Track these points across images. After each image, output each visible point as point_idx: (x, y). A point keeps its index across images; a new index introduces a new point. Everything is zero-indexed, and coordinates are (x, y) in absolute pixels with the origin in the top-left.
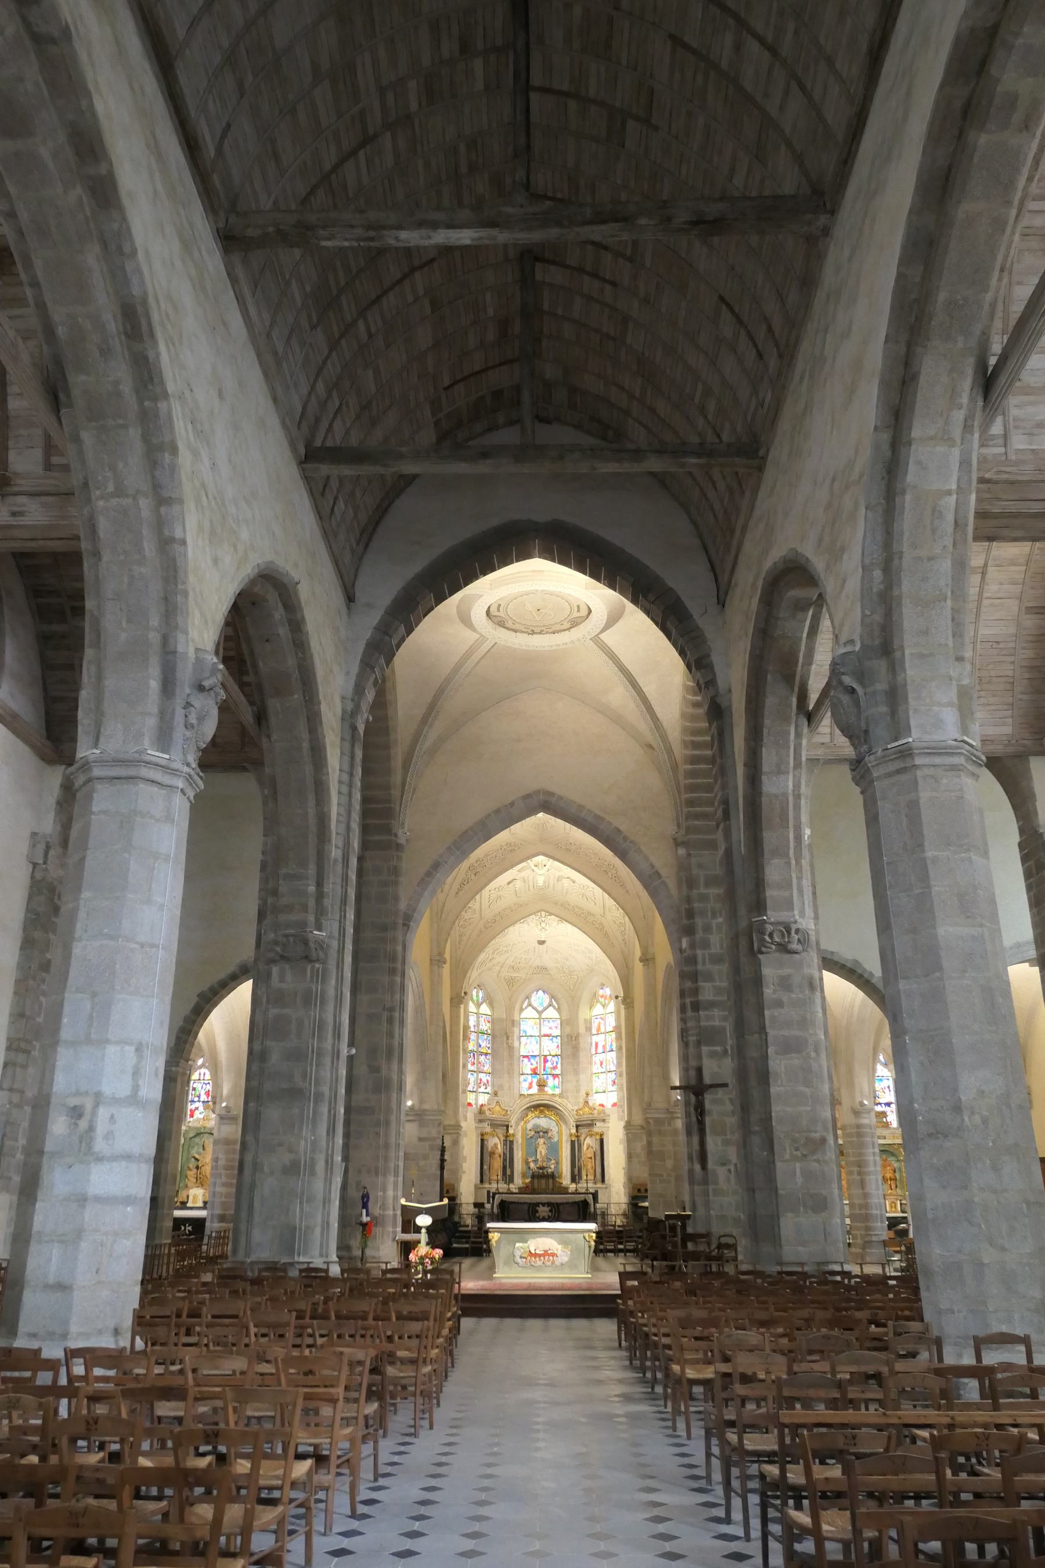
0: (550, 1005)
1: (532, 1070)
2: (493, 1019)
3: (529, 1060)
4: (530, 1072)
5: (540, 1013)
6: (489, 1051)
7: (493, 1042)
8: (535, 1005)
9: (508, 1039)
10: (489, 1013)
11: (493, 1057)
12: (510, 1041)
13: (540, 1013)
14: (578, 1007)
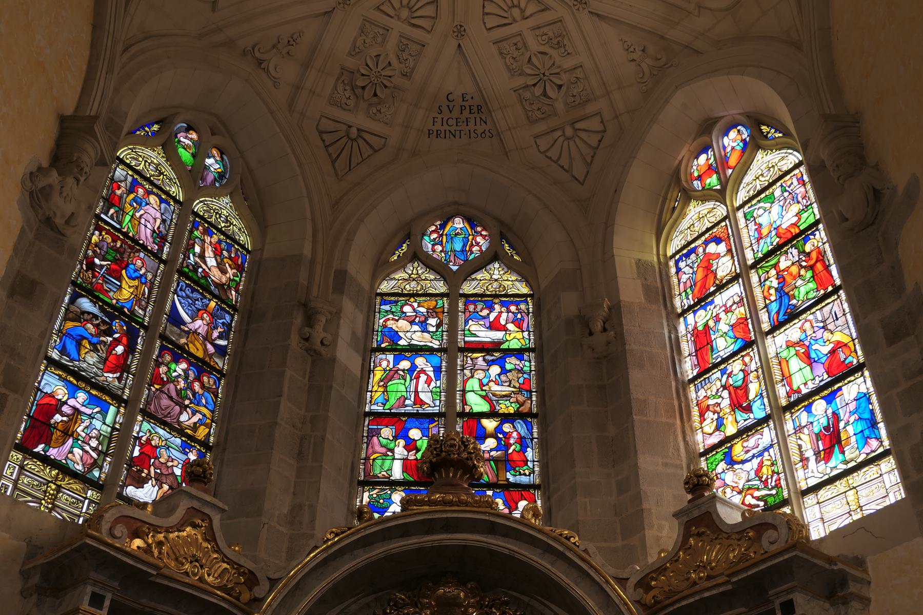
1: (407, 465)
2: (257, 265)
3: (401, 434)
4: (397, 473)
5: (453, 280)
6: (219, 363)
7: (244, 334)
9: (310, 320)
11: (233, 390)
12: (319, 333)
13: (453, 280)
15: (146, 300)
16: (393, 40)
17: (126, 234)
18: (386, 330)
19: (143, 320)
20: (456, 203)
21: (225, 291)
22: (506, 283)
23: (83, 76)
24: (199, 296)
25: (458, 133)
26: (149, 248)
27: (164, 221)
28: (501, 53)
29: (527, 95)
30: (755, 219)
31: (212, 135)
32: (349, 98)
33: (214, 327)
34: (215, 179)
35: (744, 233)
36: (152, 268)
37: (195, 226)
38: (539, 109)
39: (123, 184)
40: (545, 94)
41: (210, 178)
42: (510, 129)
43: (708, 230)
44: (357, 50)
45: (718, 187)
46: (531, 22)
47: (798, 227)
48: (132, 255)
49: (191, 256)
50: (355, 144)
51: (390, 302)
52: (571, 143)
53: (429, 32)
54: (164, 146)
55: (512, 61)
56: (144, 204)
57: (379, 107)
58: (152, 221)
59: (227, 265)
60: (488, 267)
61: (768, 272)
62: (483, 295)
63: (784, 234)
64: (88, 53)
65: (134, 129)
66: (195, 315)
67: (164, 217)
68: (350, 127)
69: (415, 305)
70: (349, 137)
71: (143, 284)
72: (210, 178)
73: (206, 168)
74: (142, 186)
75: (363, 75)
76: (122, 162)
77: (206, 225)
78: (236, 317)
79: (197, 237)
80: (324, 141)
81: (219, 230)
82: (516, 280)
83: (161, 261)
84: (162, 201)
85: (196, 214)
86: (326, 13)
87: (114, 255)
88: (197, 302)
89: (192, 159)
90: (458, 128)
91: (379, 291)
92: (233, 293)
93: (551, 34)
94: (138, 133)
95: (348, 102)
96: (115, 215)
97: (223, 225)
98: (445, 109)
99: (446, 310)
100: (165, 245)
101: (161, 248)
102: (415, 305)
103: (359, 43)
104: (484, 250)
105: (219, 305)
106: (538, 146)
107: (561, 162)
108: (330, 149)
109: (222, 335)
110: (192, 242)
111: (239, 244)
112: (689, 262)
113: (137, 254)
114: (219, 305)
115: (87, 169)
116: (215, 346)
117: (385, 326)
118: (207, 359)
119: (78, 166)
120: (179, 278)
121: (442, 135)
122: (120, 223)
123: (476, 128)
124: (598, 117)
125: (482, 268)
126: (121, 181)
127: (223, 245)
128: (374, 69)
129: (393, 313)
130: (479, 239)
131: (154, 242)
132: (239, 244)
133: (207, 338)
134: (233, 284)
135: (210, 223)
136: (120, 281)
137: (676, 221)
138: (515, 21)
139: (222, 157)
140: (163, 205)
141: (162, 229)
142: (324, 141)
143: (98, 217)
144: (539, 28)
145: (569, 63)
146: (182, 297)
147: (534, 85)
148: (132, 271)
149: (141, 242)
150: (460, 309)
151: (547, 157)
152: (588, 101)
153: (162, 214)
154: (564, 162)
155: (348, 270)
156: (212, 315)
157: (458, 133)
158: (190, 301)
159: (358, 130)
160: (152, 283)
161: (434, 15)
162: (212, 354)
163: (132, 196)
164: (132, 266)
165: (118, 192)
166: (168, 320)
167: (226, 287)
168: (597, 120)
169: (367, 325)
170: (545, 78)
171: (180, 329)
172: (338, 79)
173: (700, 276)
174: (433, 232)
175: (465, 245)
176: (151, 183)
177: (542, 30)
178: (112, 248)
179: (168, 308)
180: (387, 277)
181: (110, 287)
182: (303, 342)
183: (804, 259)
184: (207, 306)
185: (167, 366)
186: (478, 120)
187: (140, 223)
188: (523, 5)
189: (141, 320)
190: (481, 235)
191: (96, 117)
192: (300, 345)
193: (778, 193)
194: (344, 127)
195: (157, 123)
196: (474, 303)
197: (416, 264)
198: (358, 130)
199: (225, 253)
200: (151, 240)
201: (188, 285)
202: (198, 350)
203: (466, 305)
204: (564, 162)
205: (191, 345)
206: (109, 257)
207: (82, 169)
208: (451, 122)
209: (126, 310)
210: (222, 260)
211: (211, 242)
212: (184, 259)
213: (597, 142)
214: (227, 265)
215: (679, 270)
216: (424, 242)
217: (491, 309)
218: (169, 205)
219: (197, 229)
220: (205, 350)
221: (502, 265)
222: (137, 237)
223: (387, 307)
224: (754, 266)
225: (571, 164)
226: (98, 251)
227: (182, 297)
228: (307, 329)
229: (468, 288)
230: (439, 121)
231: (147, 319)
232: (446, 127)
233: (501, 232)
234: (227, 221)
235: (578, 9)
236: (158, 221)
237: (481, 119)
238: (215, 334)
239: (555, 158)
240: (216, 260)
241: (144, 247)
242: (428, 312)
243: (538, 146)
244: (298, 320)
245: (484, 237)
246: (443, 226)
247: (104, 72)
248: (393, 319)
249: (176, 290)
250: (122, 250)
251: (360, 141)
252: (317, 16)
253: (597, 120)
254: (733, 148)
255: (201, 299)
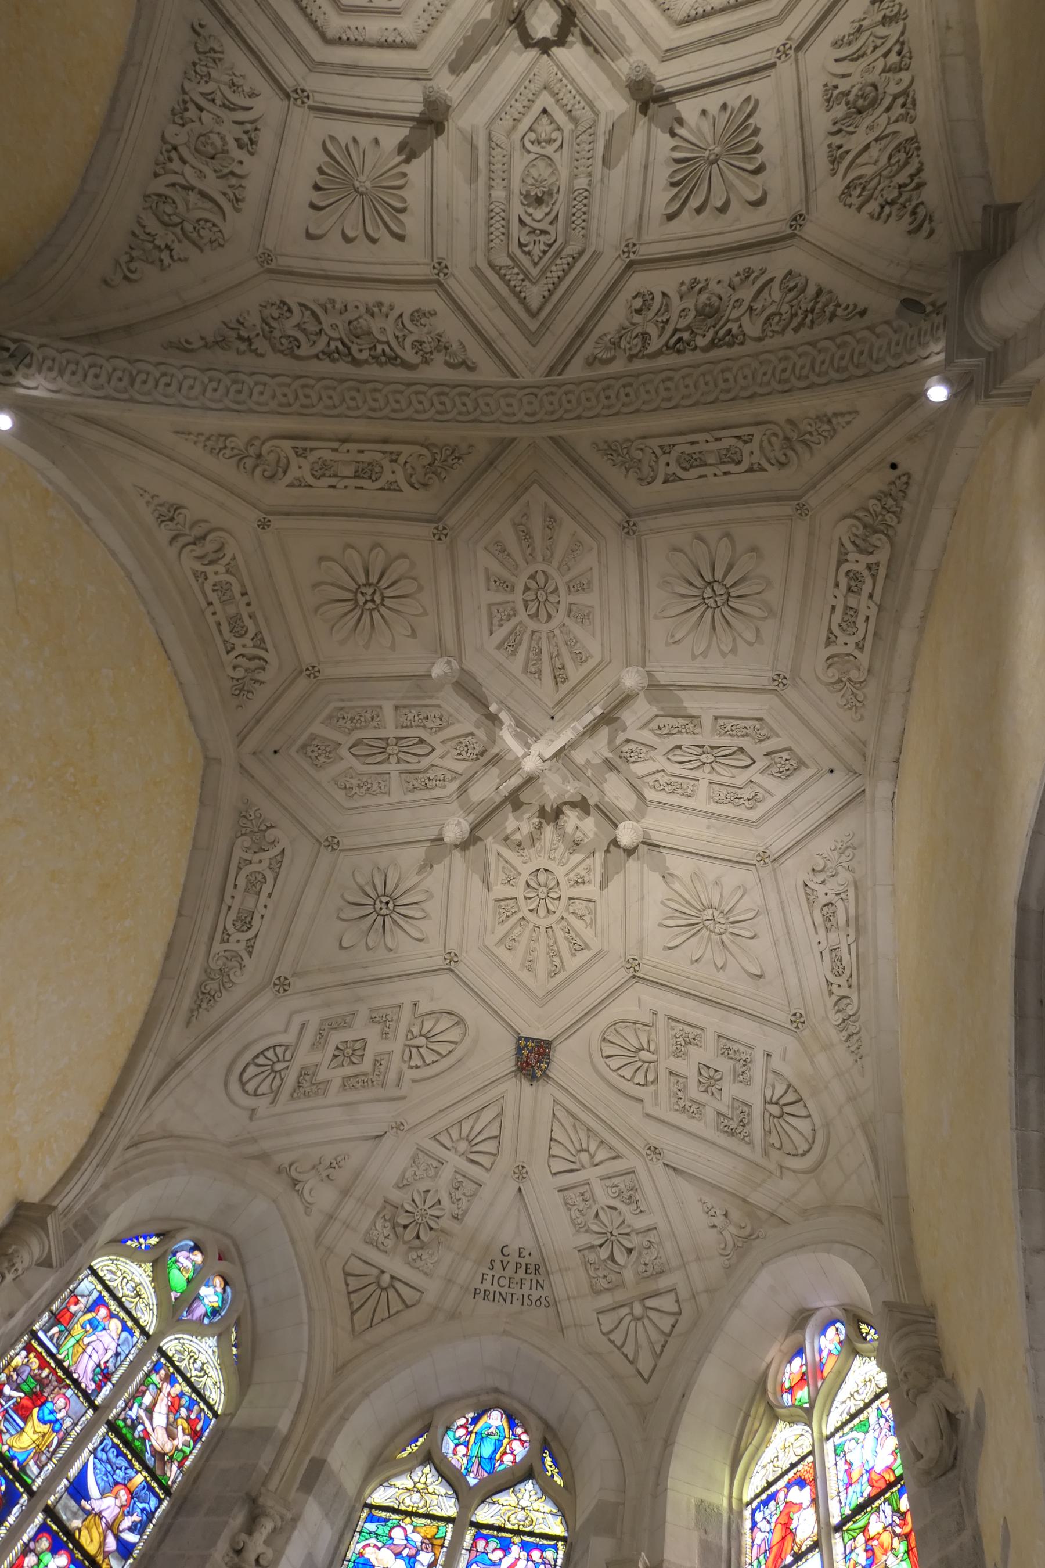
0: (527, 1472)
2: (219, 1434)
8: (458, 1459)
10: (216, 1397)
14: (668, 1443)
15: (49, 1455)
16: (447, 1174)
17: (59, 1363)
18: (361, 1561)
19: (34, 1481)
20: (496, 1390)
21: (164, 1463)
22: (534, 1515)
23: (68, 1164)
24: (125, 1464)
25: (509, 1297)
26: (83, 1386)
27: (117, 1354)
28: (566, 1204)
29: (592, 1257)
30: (845, 1455)
31: (220, 1258)
32: (387, 1237)
33: (128, 1512)
34: (206, 1314)
35: (831, 1475)
36: (76, 1413)
37: (156, 1368)
38: (605, 1277)
39: (83, 1300)
40: (612, 1257)
41: (199, 1311)
42: (569, 1298)
43: (793, 1466)
44: (405, 1182)
45: (807, 1405)
46: (601, 1170)
47: (893, 1471)
48: (57, 1390)
49: (136, 1406)
50: (384, 1294)
51: (379, 1520)
52: (640, 1324)
53: (488, 1170)
54: (155, 1263)
55: (578, 1215)
56: (100, 1328)
57: (420, 1252)
58: (101, 1351)
59: (180, 1428)
60: (517, 1488)
61: (854, 1538)
62: (500, 1529)
63: (877, 1481)
64: (84, 1140)
65: (125, 1236)
66: (108, 1489)
67: (119, 1350)
68: (383, 1272)
69: (410, 1528)
70: (379, 1286)
71: (54, 1430)
72: (199, 1311)
73: (198, 1298)
74: (107, 1306)
75: (407, 1211)
76: (94, 1273)
77: (171, 1370)
78: (165, 1503)
79: (153, 1384)
80: (347, 1285)
81: (187, 1381)
82: (551, 1512)
83: (92, 1405)
84: (125, 1328)
85: (163, 1353)
86: (378, 1136)
87: (32, 1386)
88: (118, 1471)
89: (185, 1284)
90: (511, 1291)
91: (368, 1501)
92: (175, 1468)
93: (622, 1186)
94: (129, 1243)
95: (386, 1242)
96: (56, 1336)
97: (194, 1373)
98: (497, 1265)
99: (447, 1543)
100: (105, 1384)
101: (99, 1388)
102: (410, 1528)
103: (409, 1174)
104: (518, 1460)
105: (147, 1482)
106: (600, 1324)
107: (625, 1350)
108: (352, 1296)
109: (135, 1526)
110: (143, 1388)
111: (206, 1403)
112: (767, 1512)
113: (63, 1391)
114: (147, 1482)
115: (19, 1266)
116: (119, 1540)
117: (361, 1555)
118: (100, 1559)
119: (10, 1260)
120: (107, 1433)
121: (491, 1297)
122: (58, 1347)
123: (530, 1292)
124: (673, 1294)
125: (509, 1488)
126: (83, 1296)
127: (184, 1401)
128: (420, 1207)
129: (377, 1535)
130: (516, 1445)
131: (93, 1379)
132: (206, 1403)
133: (112, 1527)
134: (179, 1456)
135: (178, 1369)
136: (25, 1420)
137: (757, 1449)
138: (583, 1167)
139: (224, 1290)
140: (125, 1334)
141: (110, 1365)
142: (347, 1285)
143: (34, 1335)
144: (609, 1178)
145: (641, 1223)
146: (101, 1460)
147: (601, 1246)
148: (46, 1411)
149: (75, 1376)
150: (465, 1544)
151: (609, 1340)
152: (662, 1272)
153: (118, 1345)
154: (629, 1350)
155: (329, 1460)
156: (132, 1495)
157: (509, 1297)
158: (109, 1468)
159: (392, 1277)
160: (67, 1433)
161: (495, 1152)
162: (110, 1553)
163: (89, 1316)
164: (49, 1405)
165: (73, 1308)
166: (67, 1489)
167: (167, 1458)
168: (671, 1297)
169: (337, 1548)
170: (613, 1238)
171: (79, 1504)
172: (378, 1213)
173: (777, 1537)
174: (462, 1426)
175: (495, 1451)
176: (121, 1305)
177: (613, 1180)
178: (34, 1377)
179: (73, 1472)
180: (385, 1482)
181: (9, 1427)
182: (231, 1554)
183: (898, 1522)
184: (130, 1479)
185: (38, 1556)
186: (534, 1282)
187: (84, 1351)
188: (592, 1150)
189: (29, 1481)
190: (520, 1440)
191: (56, 1207)
192: (227, 1559)
193: (873, 1419)
194: (375, 1272)
195: (157, 1235)
196: (486, 1538)
197: (427, 1469)
198: (392, 1277)
199: (183, 1412)
200: (90, 1375)
201: (115, 1446)
202: (92, 1541)
203: (475, 1540)
204: (629, 1350)
205: (84, 1532)
206: (25, 1388)
207: (13, 1265)
208: (503, 1282)
209: (15, 1463)
210: (175, 1420)
211: (169, 1394)
212: (124, 1409)
213: (670, 1327)
214: (180, 1428)
215: (754, 1524)
216: (446, 1438)
217: (506, 1549)
218: (132, 1335)
219: (157, 1373)
220: (103, 1543)
221: (537, 1486)
222: (72, 1369)
223: (371, 1527)
224: (838, 1528)
225: (636, 1353)
226: (15, 1377)
227: (101, 1460)
228: (244, 1536)
229: (484, 1515)
230: (490, 1278)
231: (39, 1481)
232: (496, 1287)
233: (545, 1440)
234: (202, 1369)
235: (651, 1160)
236: (110, 1353)
237: (538, 1282)
238: (127, 1523)
239: (619, 1343)
240: (168, 1418)
241: (76, 1383)
242: (422, 1543)
243: (600, 1324)
244: (238, 1519)
245: (522, 1442)
246: (475, 1421)
247: (94, 1163)
248: (375, 1546)
249: (95, 1449)
250: (46, 1381)
251: (391, 1292)
252: (367, 1138)
253: (671, 1297)
254: (830, 1353)
255: (126, 1469)
